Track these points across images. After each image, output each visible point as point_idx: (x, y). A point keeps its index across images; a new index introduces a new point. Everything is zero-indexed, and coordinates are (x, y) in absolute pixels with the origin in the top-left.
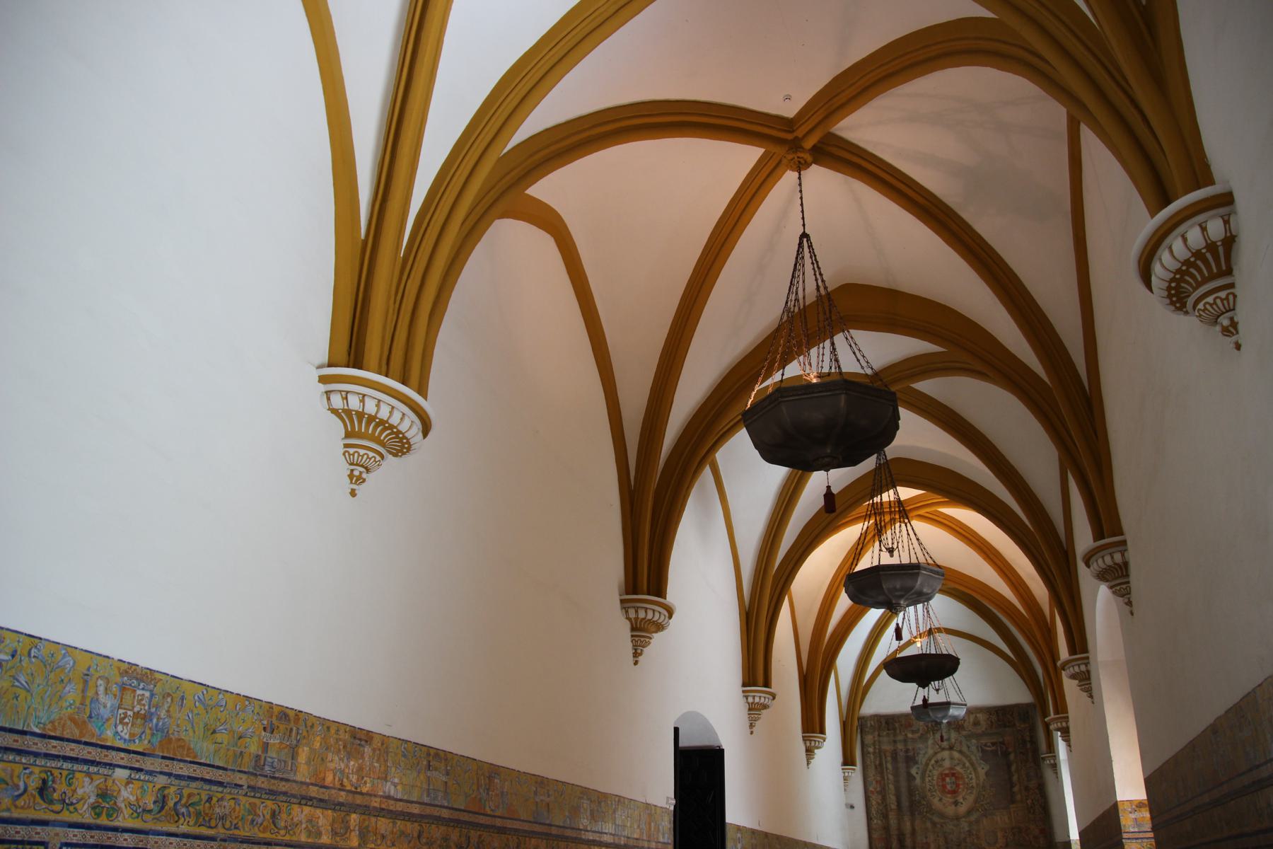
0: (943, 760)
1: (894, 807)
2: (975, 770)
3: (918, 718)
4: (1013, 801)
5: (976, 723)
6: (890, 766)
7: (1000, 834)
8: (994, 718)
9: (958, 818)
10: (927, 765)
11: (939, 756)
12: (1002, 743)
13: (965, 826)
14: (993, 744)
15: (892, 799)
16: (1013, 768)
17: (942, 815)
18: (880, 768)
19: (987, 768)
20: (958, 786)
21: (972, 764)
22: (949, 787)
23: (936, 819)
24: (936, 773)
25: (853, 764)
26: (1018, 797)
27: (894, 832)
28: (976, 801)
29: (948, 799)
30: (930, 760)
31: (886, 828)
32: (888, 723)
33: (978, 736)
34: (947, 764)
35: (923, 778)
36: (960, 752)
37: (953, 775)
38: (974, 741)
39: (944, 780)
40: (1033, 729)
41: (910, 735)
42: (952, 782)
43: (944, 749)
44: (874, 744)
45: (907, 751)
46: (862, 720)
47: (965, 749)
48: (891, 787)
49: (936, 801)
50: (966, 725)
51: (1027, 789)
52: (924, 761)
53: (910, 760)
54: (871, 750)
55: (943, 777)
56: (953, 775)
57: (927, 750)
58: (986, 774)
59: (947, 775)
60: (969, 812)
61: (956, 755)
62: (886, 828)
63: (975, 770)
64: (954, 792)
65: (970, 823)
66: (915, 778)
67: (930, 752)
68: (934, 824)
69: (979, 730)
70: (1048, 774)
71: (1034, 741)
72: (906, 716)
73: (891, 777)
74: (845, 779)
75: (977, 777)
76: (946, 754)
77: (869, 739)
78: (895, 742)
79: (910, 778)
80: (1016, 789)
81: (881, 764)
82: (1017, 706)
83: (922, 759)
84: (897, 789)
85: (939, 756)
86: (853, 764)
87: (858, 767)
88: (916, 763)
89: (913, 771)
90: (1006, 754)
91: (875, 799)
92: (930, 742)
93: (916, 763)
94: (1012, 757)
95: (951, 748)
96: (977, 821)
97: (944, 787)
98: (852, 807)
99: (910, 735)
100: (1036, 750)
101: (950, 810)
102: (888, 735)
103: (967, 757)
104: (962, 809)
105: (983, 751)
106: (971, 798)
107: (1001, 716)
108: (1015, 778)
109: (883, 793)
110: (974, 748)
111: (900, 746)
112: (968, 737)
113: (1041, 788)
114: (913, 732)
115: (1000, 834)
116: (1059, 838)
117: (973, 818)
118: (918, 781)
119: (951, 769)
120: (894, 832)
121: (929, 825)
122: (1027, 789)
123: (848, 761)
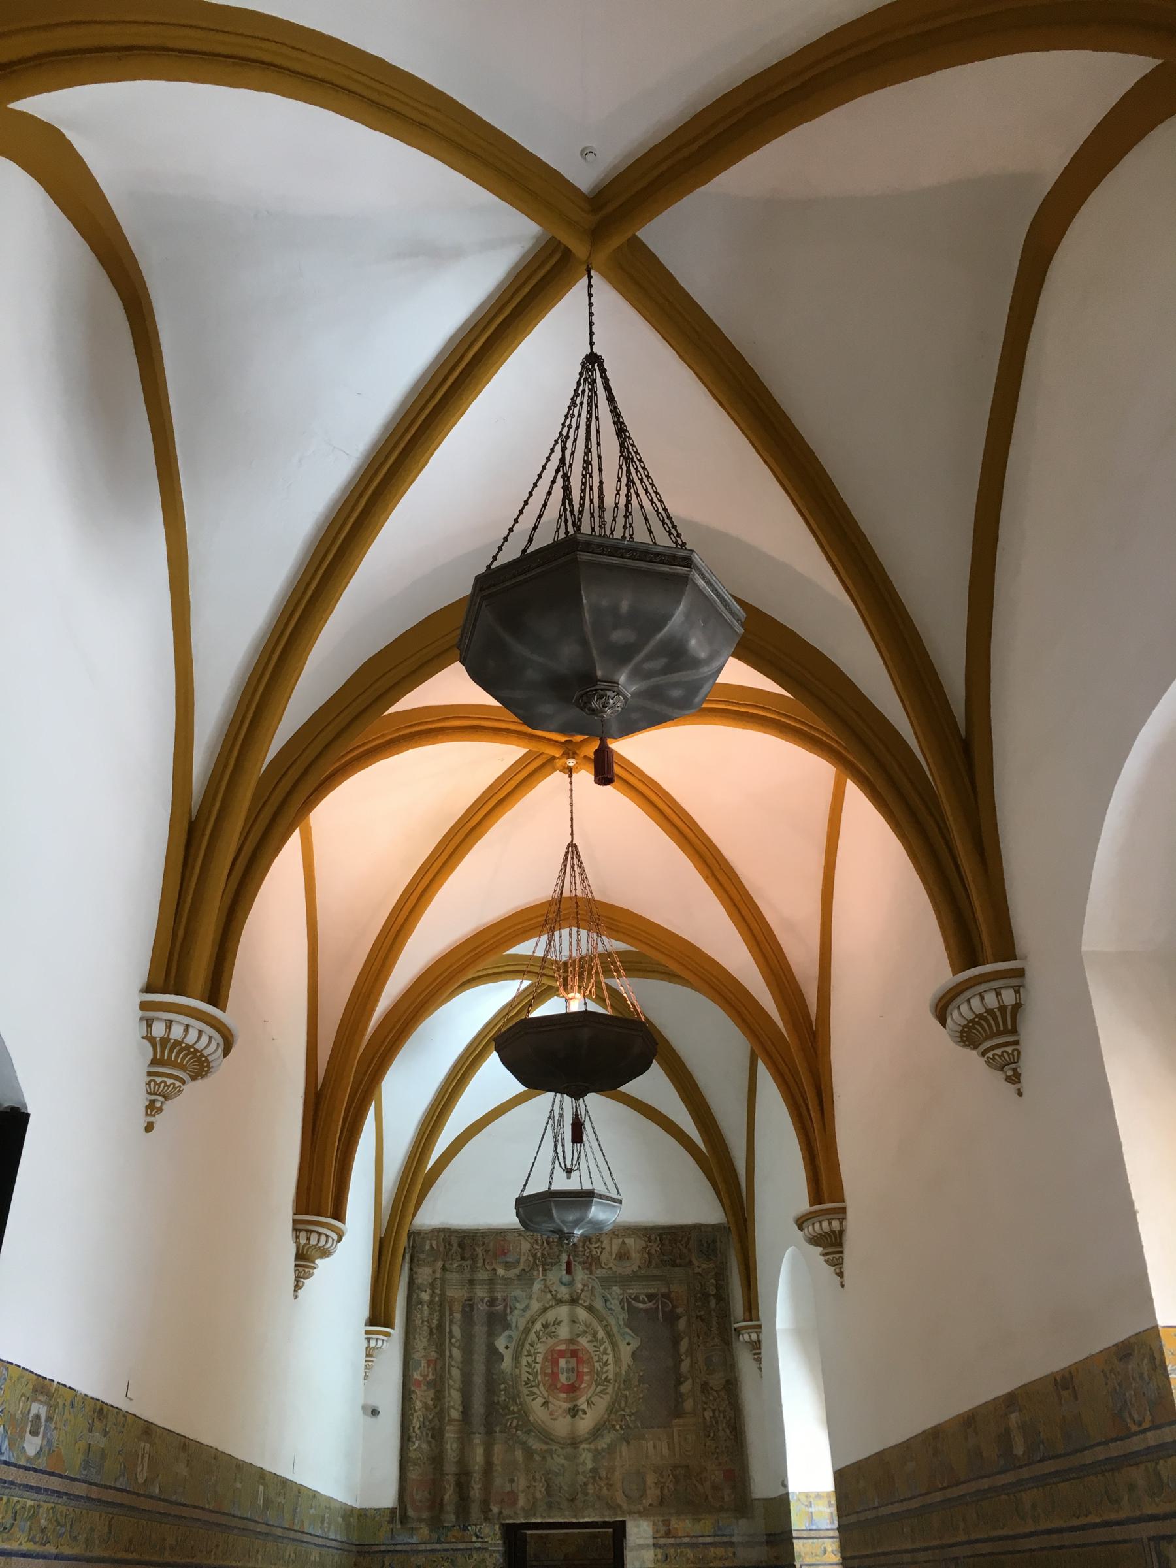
0: (557, 1323)
1: (455, 1414)
2: (614, 1345)
4: (678, 1412)
5: (623, 1256)
6: (457, 1331)
7: (651, 1479)
8: (655, 1247)
9: (574, 1442)
10: (527, 1331)
12: (666, 1296)
14: (651, 1297)
15: (454, 1397)
16: (684, 1345)
17: (547, 1436)
18: (438, 1334)
19: (635, 1343)
20: (580, 1375)
21: (609, 1335)
22: (563, 1378)
24: (541, 1348)
25: (389, 1324)
26: (688, 1405)
27: (450, 1468)
28: (611, 1410)
29: (561, 1403)
31: (437, 1460)
32: (465, 1245)
33: (625, 1281)
34: (564, 1332)
35: (516, 1359)
36: (590, 1309)
37: (574, 1353)
39: (555, 1363)
40: (721, 1274)
41: (501, 1272)
42: (569, 1370)
43: (560, 1302)
44: (432, 1286)
45: (492, 1302)
46: (416, 1237)
47: (599, 1304)
48: (456, 1372)
49: (537, 1412)
50: (603, 1258)
51: (705, 1388)
52: (522, 1323)
53: (497, 1321)
54: (425, 1296)
55: (553, 1357)
56: (574, 1353)
57: (528, 1303)
58: (634, 1354)
59: (561, 1354)
60: (596, 1433)
61: (582, 1314)
62: (437, 1460)
63: (614, 1345)
64: (572, 1389)
65: (597, 1454)
66: (501, 1357)
67: (535, 1306)
68: (529, 1453)
69: (628, 1268)
70: (745, 1360)
71: (723, 1298)
73: (457, 1353)
74: (369, 1353)
75: (617, 1361)
76: (563, 1311)
77: (424, 1274)
78: (472, 1282)
79: (493, 1355)
80: (685, 1388)
81: (440, 1326)
83: (518, 1319)
85: (550, 1316)
86: (389, 1324)
87: (397, 1332)
88: (507, 1326)
89: (500, 1343)
90: (671, 1318)
92: (537, 1286)
93: (507, 1326)
94: (682, 1324)
95: (573, 1301)
96: (611, 1449)
97: (554, 1376)
98: (375, 1412)
99: (501, 1272)
100: (725, 1315)
101: (561, 1426)
102: (461, 1269)
103: (600, 1318)
104: (585, 1424)
105: (631, 1310)
106: (602, 1404)
107: (668, 1244)
108: (685, 1366)
109: (438, 1386)
110: (614, 1304)
111: (481, 1292)
112: (606, 1282)
113: (731, 1387)
114: (508, 1266)
115: (651, 1479)
116: (761, 1489)
117: (602, 1444)
118: (507, 1364)
119: (572, 1341)
120: (450, 1468)
121: (519, 1454)
122: (705, 1388)
123: (379, 1316)
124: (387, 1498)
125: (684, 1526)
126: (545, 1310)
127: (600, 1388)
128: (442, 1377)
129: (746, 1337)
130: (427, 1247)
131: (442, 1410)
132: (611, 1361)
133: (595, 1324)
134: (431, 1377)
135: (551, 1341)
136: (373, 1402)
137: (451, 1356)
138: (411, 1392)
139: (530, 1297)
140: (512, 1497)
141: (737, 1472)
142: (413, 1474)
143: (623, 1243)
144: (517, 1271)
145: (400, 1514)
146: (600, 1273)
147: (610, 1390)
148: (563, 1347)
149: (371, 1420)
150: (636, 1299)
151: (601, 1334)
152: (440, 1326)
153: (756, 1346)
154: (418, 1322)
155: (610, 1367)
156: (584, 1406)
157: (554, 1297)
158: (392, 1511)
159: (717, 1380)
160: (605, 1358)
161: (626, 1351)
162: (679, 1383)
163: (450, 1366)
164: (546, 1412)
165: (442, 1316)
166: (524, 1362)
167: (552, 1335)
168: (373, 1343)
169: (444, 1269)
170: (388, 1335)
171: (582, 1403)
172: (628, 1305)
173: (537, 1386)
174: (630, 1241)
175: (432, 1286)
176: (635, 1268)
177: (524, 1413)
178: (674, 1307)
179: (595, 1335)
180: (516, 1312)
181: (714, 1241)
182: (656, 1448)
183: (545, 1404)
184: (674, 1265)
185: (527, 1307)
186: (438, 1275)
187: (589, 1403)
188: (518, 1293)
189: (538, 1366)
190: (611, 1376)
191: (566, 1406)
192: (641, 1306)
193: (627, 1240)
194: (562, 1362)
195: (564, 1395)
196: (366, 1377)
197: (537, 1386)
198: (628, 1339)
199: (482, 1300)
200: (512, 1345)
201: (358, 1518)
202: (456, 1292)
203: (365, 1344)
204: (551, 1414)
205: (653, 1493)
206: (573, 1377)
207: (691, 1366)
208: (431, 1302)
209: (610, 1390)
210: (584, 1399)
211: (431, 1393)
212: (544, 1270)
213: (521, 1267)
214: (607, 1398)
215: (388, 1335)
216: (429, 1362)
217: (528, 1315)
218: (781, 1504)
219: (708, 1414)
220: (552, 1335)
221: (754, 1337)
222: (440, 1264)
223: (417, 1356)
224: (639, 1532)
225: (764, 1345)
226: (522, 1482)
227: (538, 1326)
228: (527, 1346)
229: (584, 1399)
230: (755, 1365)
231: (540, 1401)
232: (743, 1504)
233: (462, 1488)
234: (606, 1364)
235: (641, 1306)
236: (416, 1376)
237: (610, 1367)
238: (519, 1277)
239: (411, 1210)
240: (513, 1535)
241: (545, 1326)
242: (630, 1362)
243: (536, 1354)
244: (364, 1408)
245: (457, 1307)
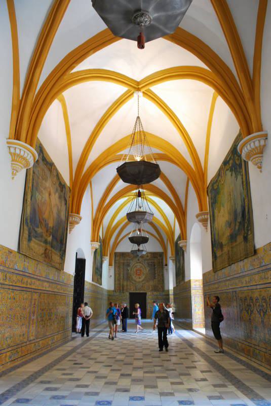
1: (122, 278)
3: (132, 254)
4: (155, 278)
5: (147, 256)
11: (136, 265)
13: (141, 284)
15: (122, 276)
16: (156, 269)
17: (135, 281)
23: (134, 282)
24: (135, 269)
25: (112, 265)
26: (156, 277)
27: (121, 285)
28: (145, 277)
31: (120, 284)
35: (131, 270)
36: (142, 264)
38: (146, 261)
40: (162, 259)
43: (137, 263)
46: (115, 253)
49: (134, 277)
51: (159, 275)
52: (132, 266)
53: (128, 265)
55: (137, 270)
57: (132, 263)
58: (149, 270)
60: (143, 281)
61: (141, 265)
62: (120, 284)
65: (143, 284)
68: (133, 283)
69: (148, 258)
71: (162, 263)
72: (128, 253)
74: (109, 269)
76: (139, 264)
77: (117, 258)
80: (156, 275)
82: (159, 253)
84: (123, 274)
85: (136, 265)
87: (113, 266)
89: (129, 268)
90: (154, 265)
91: (117, 276)
94: (156, 266)
95: (140, 263)
96: (145, 283)
97: (137, 273)
100: (163, 265)
101: (138, 280)
104: (141, 280)
107: (154, 255)
108: (156, 272)
109: (119, 274)
111: (125, 261)
113: (163, 275)
116: (166, 288)
117: (143, 282)
118: (130, 271)
120: (121, 285)
123: (110, 264)
124: (112, 288)
125: (155, 293)
133: (143, 266)
140: (131, 289)
141: (163, 287)
142: (116, 286)
145: (115, 291)
153: (167, 270)
158: (113, 291)
159: (161, 274)
161: (147, 270)
164: (135, 277)
172: (148, 264)
177: (132, 278)
182: (151, 283)
201: (109, 291)
202: (122, 261)
205: (151, 289)
218: (168, 291)
224: (149, 294)
226: (132, 287)
232: (163, 290)
233: (123, 288)
240: (131, 294)
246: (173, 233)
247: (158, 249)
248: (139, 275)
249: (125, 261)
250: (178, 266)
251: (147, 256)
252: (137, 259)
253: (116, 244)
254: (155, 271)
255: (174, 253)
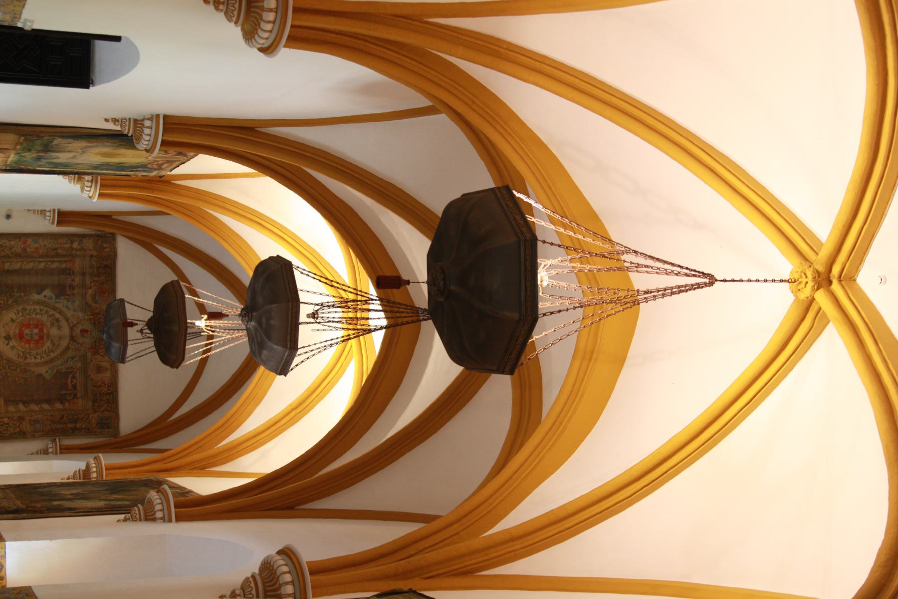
0: (59, 328)
1: (7, 266)
2: (46, 363)
4: (7, 402)
5: (99, 369)
6: (55, 265)
10: (55, 309)
11: (63, 323)
12: (75, 396)
14: (74, 387)
16: (46, 406)
19: (48, 377)
20: (28, 342)
21: (52, 360)
22: (27, 331)
24: (44, 318)
25: (59, 223)
26: (12, 409)
28: (9, 361)
29: (13, 330)
30: (60, 313)
32: (107, 269)
34: (54, 331)
35: (39, 302)
36: (67, 348)
37: (41, 338)
38: (79, 365)
39: (36, 326)
40: (89, 432)
41: (90, 292)
43: (72, 329)
44: (82, 249)
45: (72, 287)
46: (113, 237)
47: (70, 353)
48: (31, 265)
50: (98, 356)
51: (21, 419)
52: (59, 306)
53: (61, 291)
54: (75, 245)
55: (39, 325)
56: (41, 338)
58: (40, 375)
59: (41, 330)
61: (65, 343)
64: (21, 336)
66: (39, 293)
67: (69, 314)
71: (74, 432)
72: (113, 290)
73: (42, 265)
74: (43, 212)
75: (37, 365)
76: (66, 331)
77: (89, 244)
78: (83, 274)
79: (40, 289)
80: (21, 407)
81: (58, 255)
82: (117, 417)
83: (61, 304)
84: (28, 272)
85: (63, 323)
86: (59, 223)
87: (55, 229)
89: (48, 292)
90: (62, 399)
91: (18, 246)
92: (80, 314)
93: (57, 297)
94: (58, 406)
95: (72, 338)
97: (28, 326)
98: (8, 217)
99: (90, 292)
100: (65, 433)
103: (62, 354)
106: (12, 355)
107: (108, 397)
108: (34, 407)
111: (78, 279)
113: (21, 435)
114: (93, 296)
118: (36, 297)
119: (48, 336)
122: (21, 419)
123: (64, 217)
126: (67, 320)
127: (21, 354)
128: (28, 256)
129: (50, 446)
130: (105, 245)
131: (9, 257)
132: (37, 361)
133: (59, 351)
134: (29, 250)
135: (48, 324)
136: (14, 215)
137: (40, 262)
138: (20, 238)
139: (75, 311)
143: (107, 369)
144: (90, 302)
146: (89, 354)
147: (20, 360)
148: (45, 331)
149: (4, 213)
150: (74, 377)
151: (52, 355)
152: (58, 255)
153: (45, 452)
154: (60, 241)
155: (33, 360)
156: (11, 344)
157: (75, 325)
159: (26, 426)
160: (39, 357)
161: (42, 370)
162: (24, 403)
163: (35, 262)
165: (64, 256)
166: (37, 307)
167: (52, 324)
168: (48, 214)
169: (92, 256)
170: (53, 223)
171: (13, 343)
173: (23, 315)
174: (108, 374)
175: (82, 249)
176: (92, 376)
178: (69, 401)
179: (52, 351)
180: (66, 302)
181: (108, 427)
183: (13, 321)
184: (94, 402)
185: (69, 309)
186: (88, 252)
187: (13, 347)
188: (77, 303)
189: (34, 316)
190: (28, 361)
191: (11, 333)
192: (69, 380)
193: (109, 372)
194: (36, 331)
195: (17, 331)
196: (29, 210)
197: (23, 315)
198: (50, 372)
199: (73, 280)
200: (46, 299)
202: (77, 265)
203: (48, 209)
204: (7, 324)
206: (28, 338)
207: (34, 411)
208: (72, 249)
209: (20, 360)
210: (15, 344)
211: (19, 251)
212: (91, 319)
213: (93, 305)
214: (16, 358)
215: (53, 223)
216: (37, 249)
217: (64, 309)
219: (6, 420)
220: (52, 324)
221: (50, 450)
222: (95, 253)
223: (41, 241)
225: (46, 456)
227: (58, 316)
228: (46, 309)
229: (15, 344)
230: (35, 450)
231: (14, 317)
234: (35, 358)
235: (69, 380)
236: (29, 241)
237: (33, 360)
238: (87, 303)
239: (130, 235)
241: (57, 320)
242: (36, 373)
243: (42, 314)
244: (10, 210)
245: (69, 265)
246: (201, 468)
247: (133, 413)
248: (21, 336)
249: (78, 279)
250: (66, 492)
251: (99, 369)
252: (87, 326)
253: (149, 240)
254: (38, 402)
255: (118, 476)
